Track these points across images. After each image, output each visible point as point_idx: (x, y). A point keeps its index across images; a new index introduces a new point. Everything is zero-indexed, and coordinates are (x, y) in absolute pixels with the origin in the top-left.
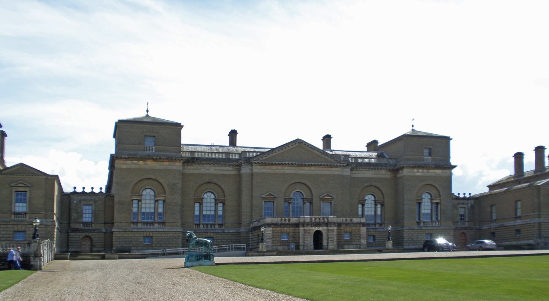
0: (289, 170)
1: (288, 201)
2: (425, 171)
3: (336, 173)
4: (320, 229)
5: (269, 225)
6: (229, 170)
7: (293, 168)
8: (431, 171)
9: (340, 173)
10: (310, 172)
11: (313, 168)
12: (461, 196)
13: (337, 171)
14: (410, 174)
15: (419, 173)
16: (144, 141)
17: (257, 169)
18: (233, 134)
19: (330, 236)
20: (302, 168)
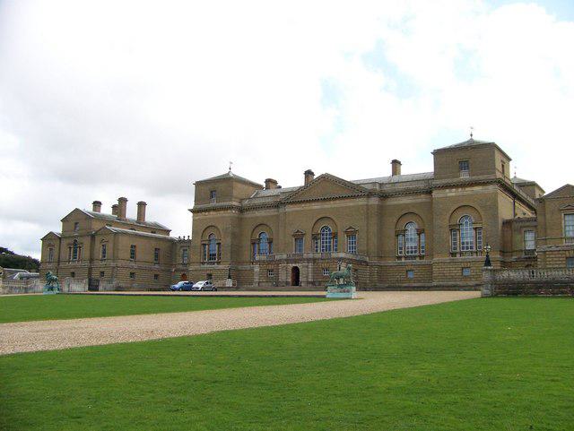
0: (316, 206)
1: (315, 237)
2: (460, 189)
3: (360, 203)
4: (297, 265)
5: (257, 262)
6: (272, 212)
7: (319, 203)
8: (467, 189)
9: (365, 203)
10: (336, 206)
11: (338, 201)
12: (186, 239)
13: (361, 202)
14: (441, 195)
15: (452, 193)
16: (215, 194)
17: (289, 209)
18: (396, 164)
19: (306, 273)
20: (328, 203)
